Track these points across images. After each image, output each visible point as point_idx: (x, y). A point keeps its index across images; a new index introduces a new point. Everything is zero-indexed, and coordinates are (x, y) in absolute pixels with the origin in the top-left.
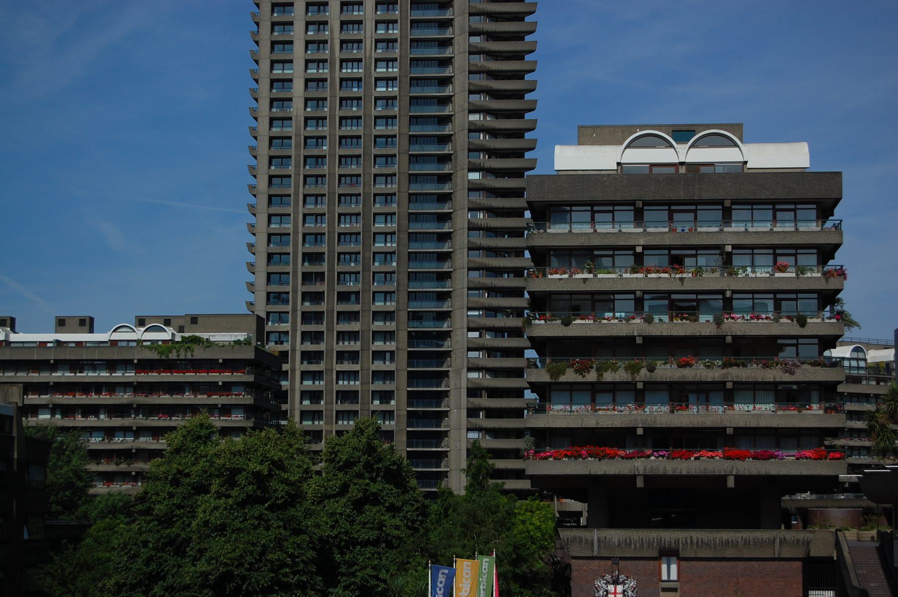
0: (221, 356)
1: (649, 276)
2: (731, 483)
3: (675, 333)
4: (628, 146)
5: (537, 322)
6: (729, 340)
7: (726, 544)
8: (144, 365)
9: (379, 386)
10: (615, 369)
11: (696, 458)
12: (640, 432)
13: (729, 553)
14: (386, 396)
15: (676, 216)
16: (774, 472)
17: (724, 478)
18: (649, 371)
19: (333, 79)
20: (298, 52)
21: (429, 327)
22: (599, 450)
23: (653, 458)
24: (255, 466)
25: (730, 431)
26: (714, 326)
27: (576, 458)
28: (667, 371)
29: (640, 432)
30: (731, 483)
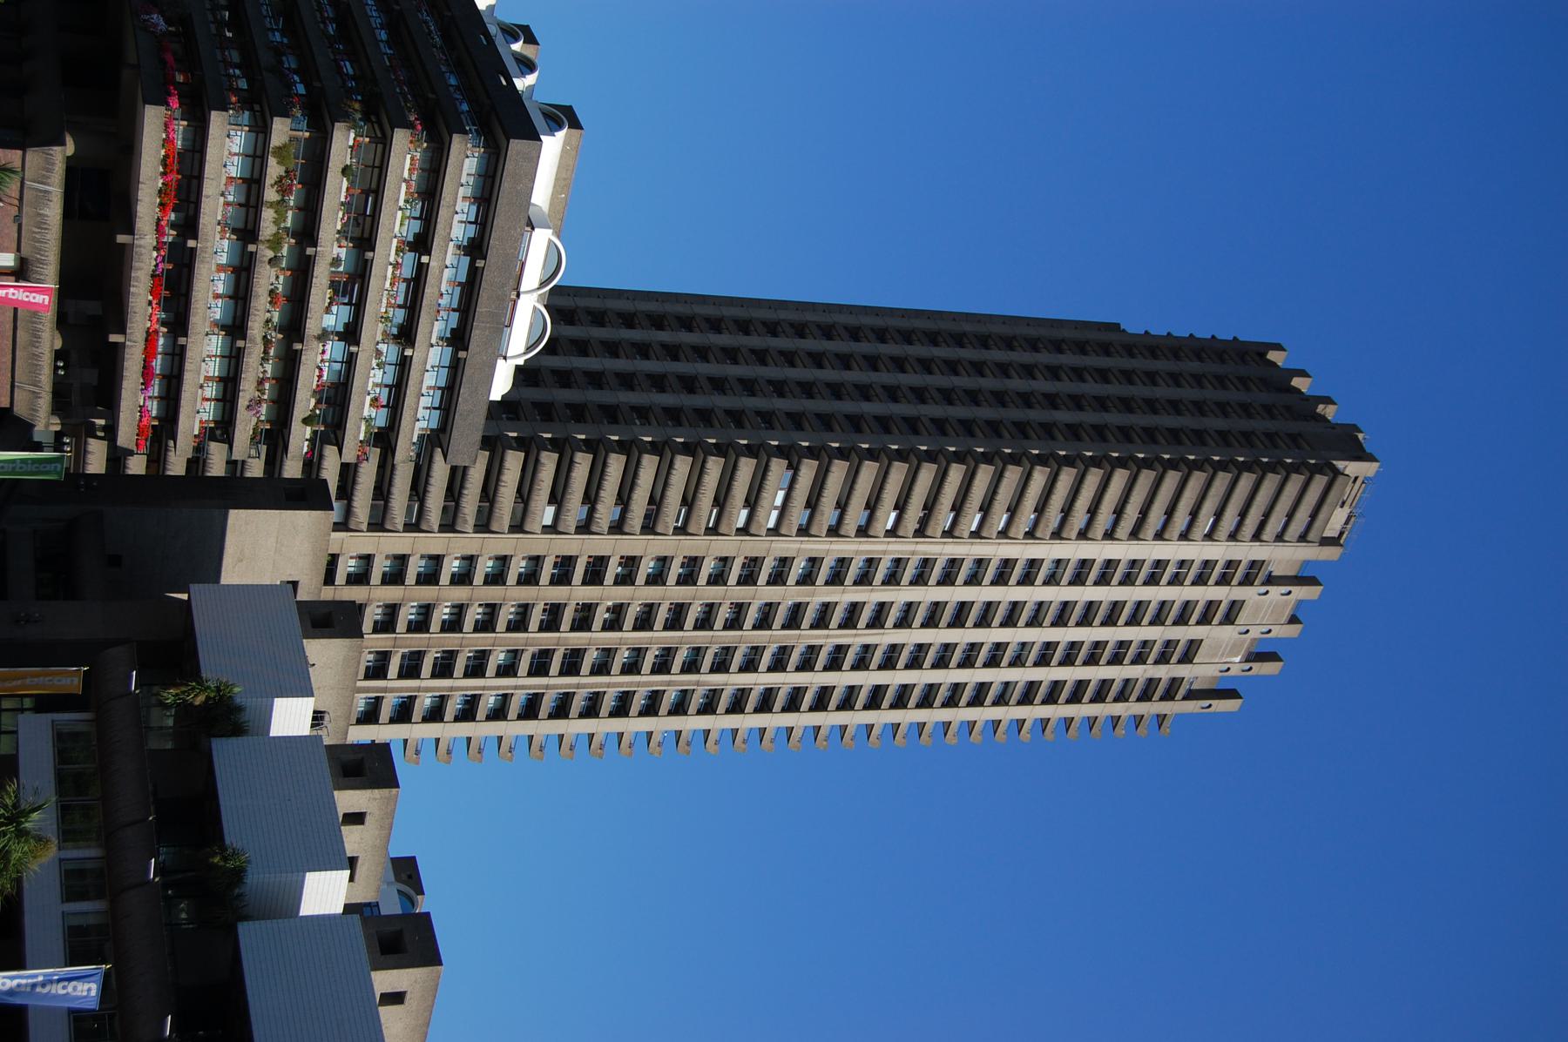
1: (390, 269)
2: (113, 338)
3: (313, 291)
5: (352, 135)
6: (297, 346)
7: (35, 336)
10: (276, 222)
11: (150, 303)
12: (191, 243)
13: (22, 335)
16: (125, 384)
17: (122, 329)
18: (273, 262)
23: (155, 254)
25: (182, 340)
26: (318, 332)
27: (165, 166)
28: (269, 279)
30: (113, 338)
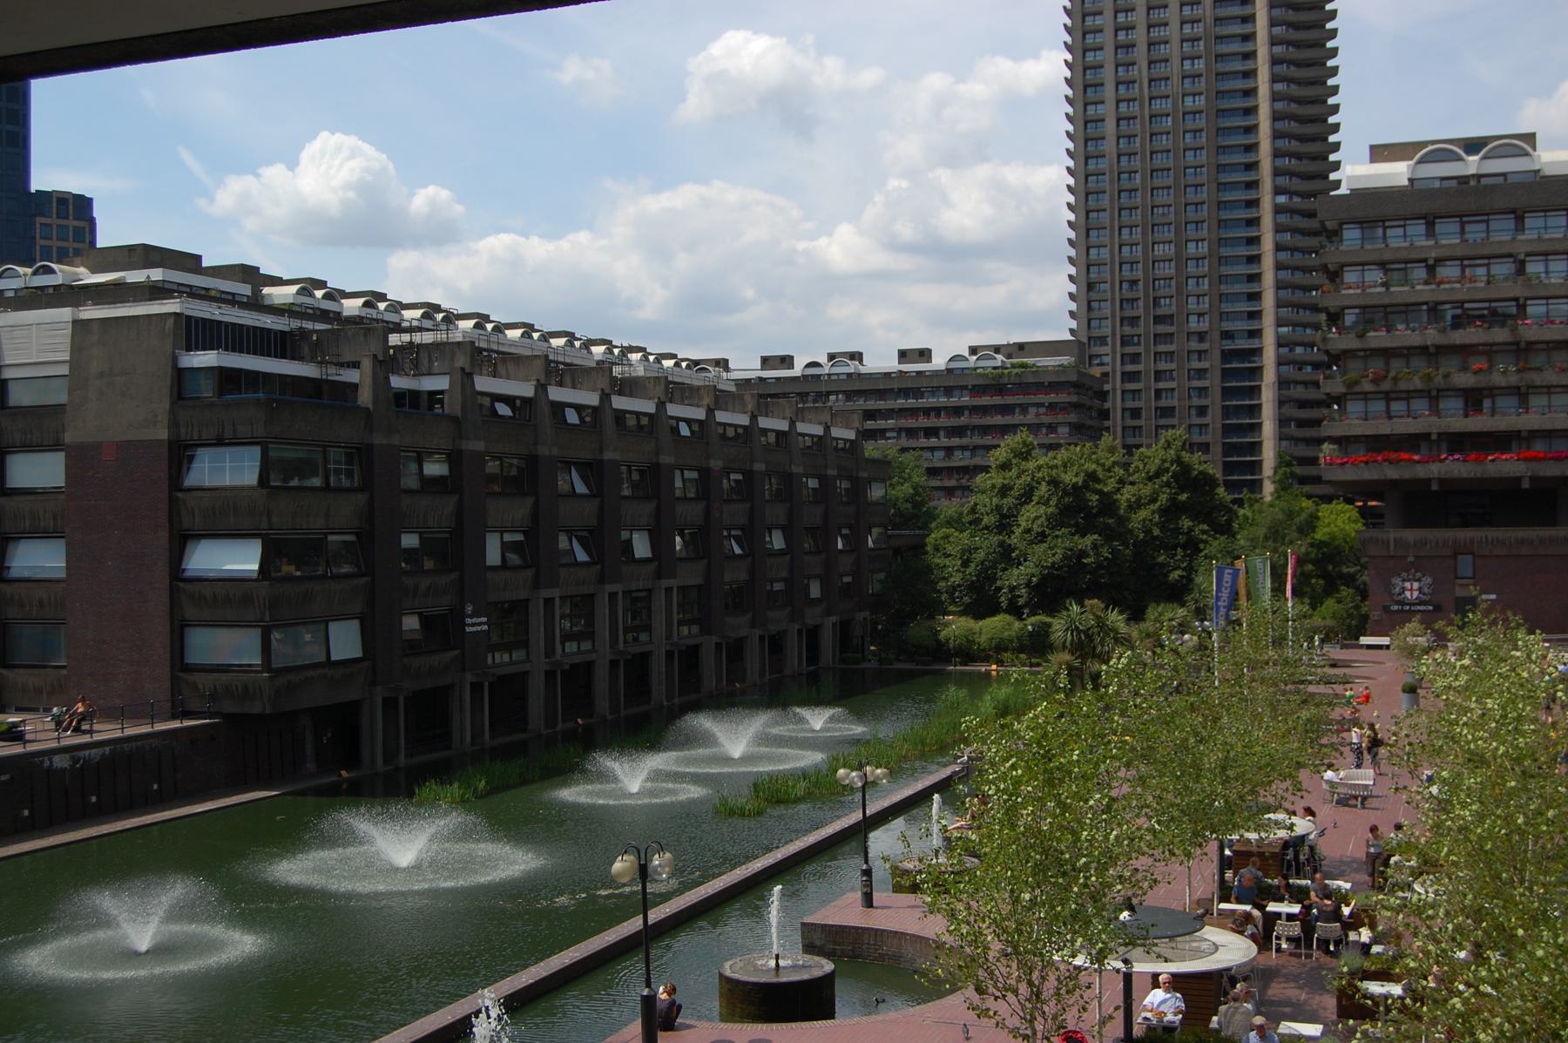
0: (1046, 379)
2: (1526, 485)
4: (1419, 162)
7: (1522, 541)
8: (977, 390)
9: (1196, 401)
12: (1434, 437)
14: (1202, 411)
15: (1468, 228)
17: (1519, 479)
19: (1142, 116)
20: (1109, 92)
21: (1242, 344)
22: (1394, 456)
24: (1069, 478)
29: (1434, 437)
30: (1526, 485)
